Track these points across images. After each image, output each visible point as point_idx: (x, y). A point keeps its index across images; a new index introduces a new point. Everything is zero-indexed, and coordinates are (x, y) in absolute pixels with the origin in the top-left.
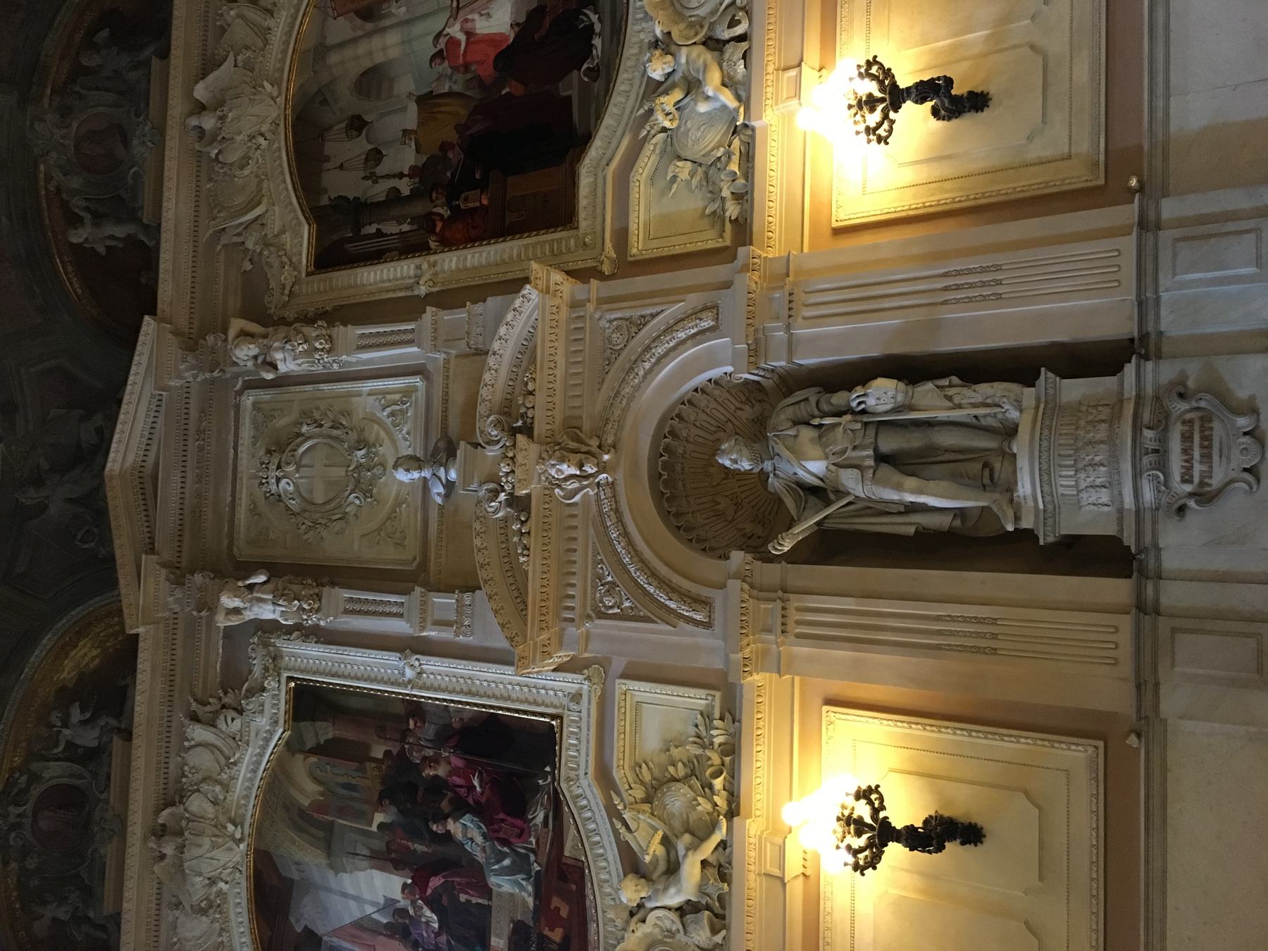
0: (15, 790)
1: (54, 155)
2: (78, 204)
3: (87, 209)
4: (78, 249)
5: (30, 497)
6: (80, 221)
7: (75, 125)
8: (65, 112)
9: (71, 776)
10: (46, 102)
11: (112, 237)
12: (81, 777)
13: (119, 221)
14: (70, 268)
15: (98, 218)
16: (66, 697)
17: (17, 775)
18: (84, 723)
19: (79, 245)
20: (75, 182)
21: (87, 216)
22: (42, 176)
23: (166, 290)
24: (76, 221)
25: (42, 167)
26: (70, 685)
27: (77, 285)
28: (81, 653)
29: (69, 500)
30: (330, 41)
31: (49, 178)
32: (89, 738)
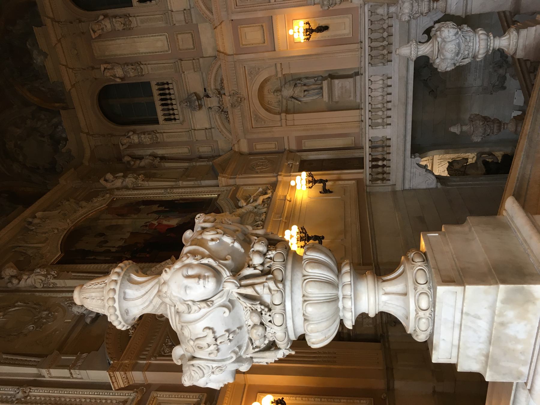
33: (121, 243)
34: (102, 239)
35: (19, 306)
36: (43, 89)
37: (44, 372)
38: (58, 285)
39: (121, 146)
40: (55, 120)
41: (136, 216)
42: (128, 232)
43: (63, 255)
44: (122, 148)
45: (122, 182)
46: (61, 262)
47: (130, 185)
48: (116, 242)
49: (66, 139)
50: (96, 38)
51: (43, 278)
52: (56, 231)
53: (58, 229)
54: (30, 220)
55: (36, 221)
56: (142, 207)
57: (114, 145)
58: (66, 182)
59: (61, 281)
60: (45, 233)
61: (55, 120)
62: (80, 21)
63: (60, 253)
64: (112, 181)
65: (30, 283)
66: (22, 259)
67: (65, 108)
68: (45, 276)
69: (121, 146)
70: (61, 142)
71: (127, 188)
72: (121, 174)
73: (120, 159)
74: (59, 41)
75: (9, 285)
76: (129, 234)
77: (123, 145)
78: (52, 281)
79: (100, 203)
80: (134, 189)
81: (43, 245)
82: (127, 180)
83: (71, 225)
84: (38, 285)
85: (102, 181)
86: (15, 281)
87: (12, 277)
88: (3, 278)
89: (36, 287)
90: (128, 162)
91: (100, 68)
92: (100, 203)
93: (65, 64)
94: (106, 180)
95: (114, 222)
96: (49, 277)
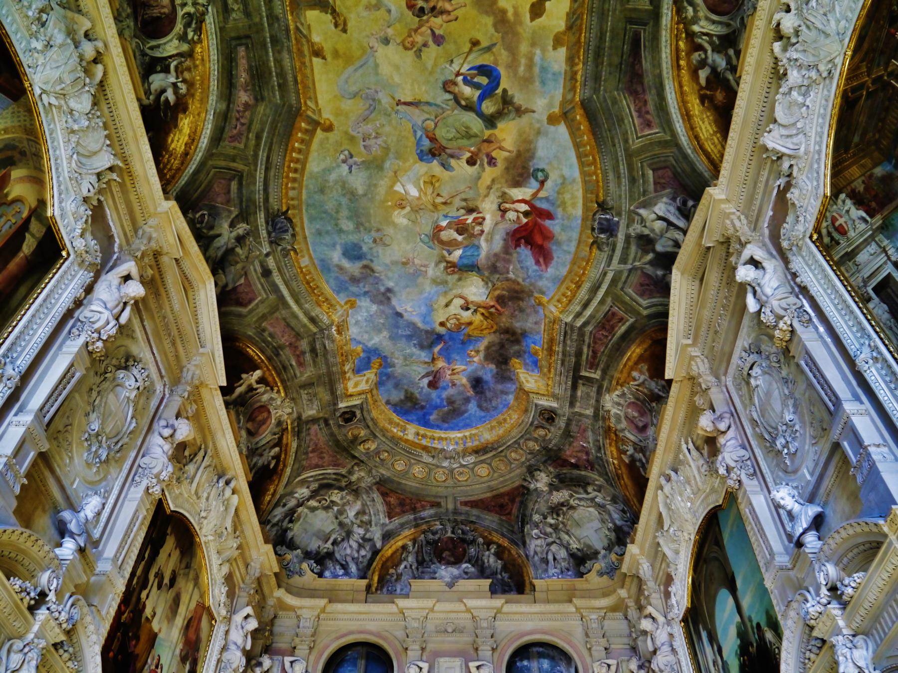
0: (193, 25)
1: (279, 403)
2: (262, 388)
3: (256, 389)
4: (255, 367)
5: (242, 228)
6: (258, 382)
7: (273, 421)
8: (279, 423)
9: (158, 46)
10: (289, 422)
11: (241, 385)
12: (152, 48)
13: (240, 395)
14: (256, 357)
15: (251, 389)
16: (181, 106)
17: (196, 38)
18: (163, 91)
19: (254, 371)
20: (265, 397)
21: (255, 386)
22: (282, 391)
23: (219, 401)
24: (261, 381)
25: (283, 394)
26: (181, 116)
27: (250, 351)
28: (181, 141)
29: (219, 235)
30: (196, 589)
31: (278, 392)
32: (157, 80)
33: (148, 612)
34: (166, 581)
35: (130, 423)
36: (402, 566)
37: (27, 418)
38: (132, 489)
39: (292, 659)
40: (353, 568)
41: (178, 652)
42: (160, 631)
43: (168, 512)
44: (287, 660)
45: (236, 644)
46: (160, 506)
47: (226, 656)
48: (154, 602)
49: (320, 575)
50: (467, 667)
51: (155, 471)
52: (203, 514)
53: (205, 518)
54: (232, 484)
55: (228, 492)
56: (188, 667)
57: (295, 648)
58: (263, 556)
59: (140, 495)
60: (207, 499)
61: (353, 568)
62: (493, 649)
63: (172, 509)
64: (242, 628)
65: (153, 451)
66: (187, 453)
67: (369, 587)
68: (157, 476)
69: (292, 659)
70: (319, 567)
71: (224, 649)
72: (248, 647)
73: (267, 650)
74: (468, 610)
75: (163, 423)
76: (156, 630)
77: (292, 662)
78: (145, 483)
79: (216, 596)
80: (219, 661)
81: (193, 492)
82: (239, 654)
83: (203, 539)
84: (146, 460)
85: (249, 610)
86: (167, 432)
87: (175, 431)
88: (177, 419)
89: (143, 456)
90: (260, 664)
91: (421, 660)
92: (216, 596)
93: (435, 608)
94: (246, 617)
95: (182, 610)
96: (154, 481)
